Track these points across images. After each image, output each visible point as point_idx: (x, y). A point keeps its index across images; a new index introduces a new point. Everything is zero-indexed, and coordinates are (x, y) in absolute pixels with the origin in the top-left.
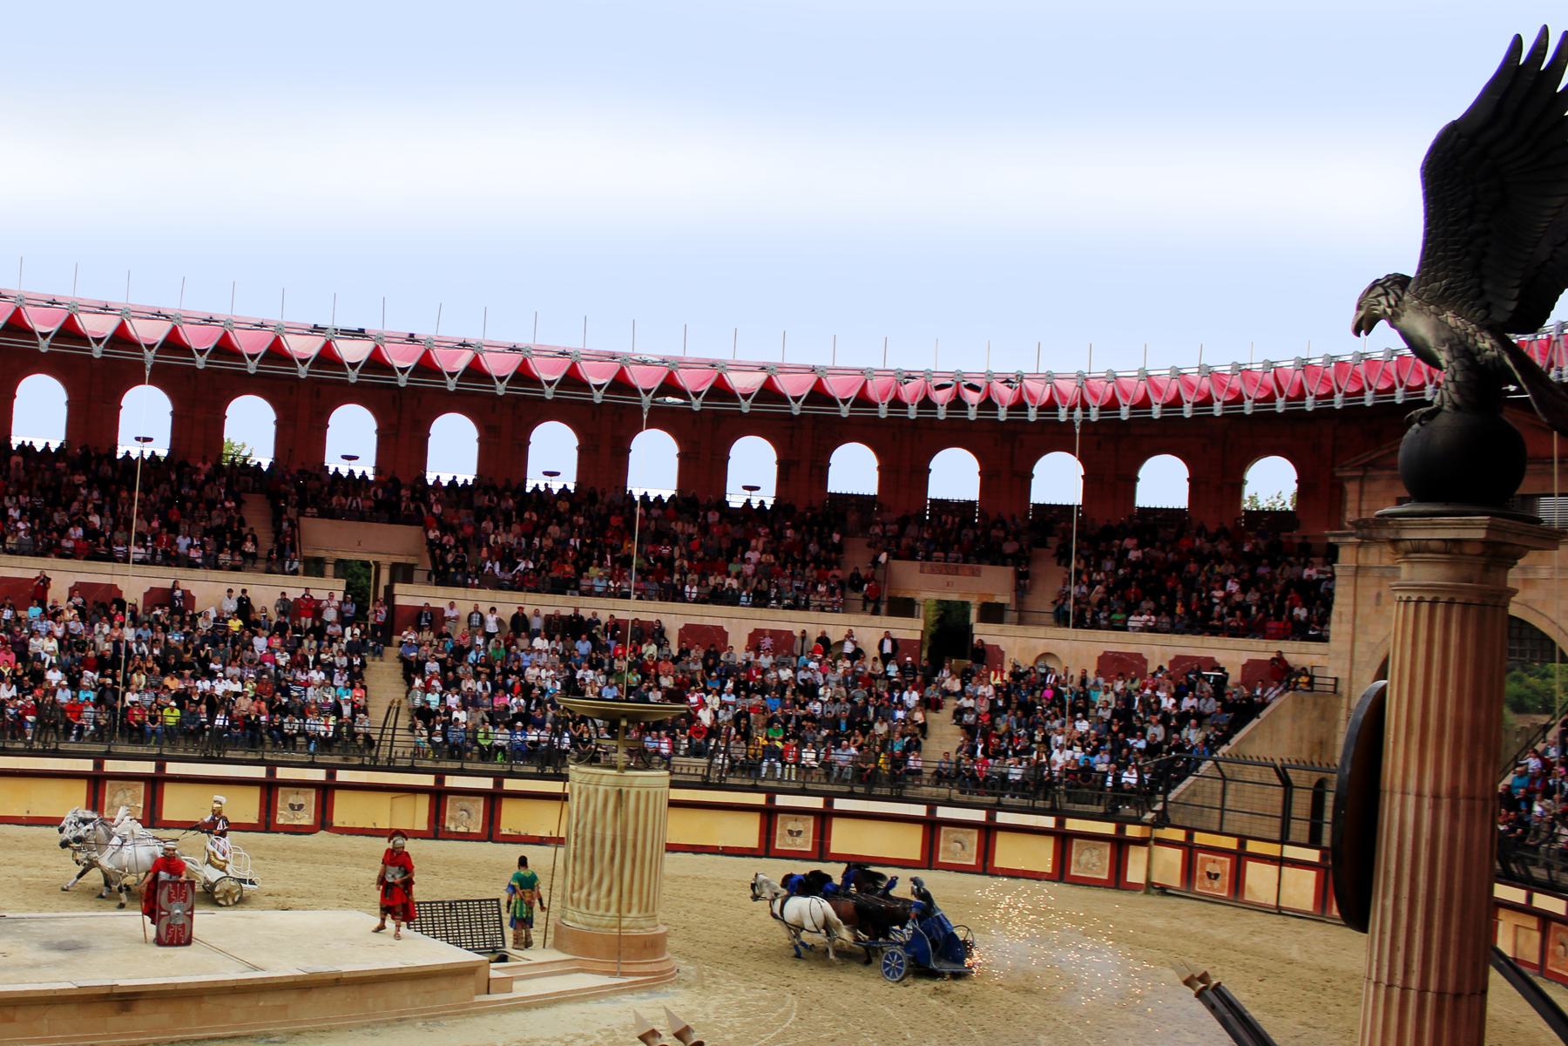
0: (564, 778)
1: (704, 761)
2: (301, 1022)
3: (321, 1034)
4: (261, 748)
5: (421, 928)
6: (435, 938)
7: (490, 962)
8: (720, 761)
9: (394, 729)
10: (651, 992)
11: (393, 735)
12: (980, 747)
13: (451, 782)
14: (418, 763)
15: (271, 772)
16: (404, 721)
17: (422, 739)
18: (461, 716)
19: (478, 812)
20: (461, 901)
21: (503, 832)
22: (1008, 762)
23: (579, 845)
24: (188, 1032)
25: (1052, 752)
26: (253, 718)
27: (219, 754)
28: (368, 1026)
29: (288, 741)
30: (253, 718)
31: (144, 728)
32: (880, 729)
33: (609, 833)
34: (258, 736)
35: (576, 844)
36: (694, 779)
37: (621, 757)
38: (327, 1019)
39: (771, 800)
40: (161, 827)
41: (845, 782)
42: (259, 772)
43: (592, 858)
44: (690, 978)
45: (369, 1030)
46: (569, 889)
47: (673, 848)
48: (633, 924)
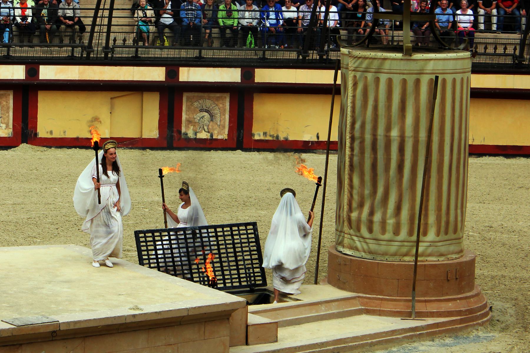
0: (335, 65)
5: (158, 263)
7: (248, 304)
9: (111, 9)
10: (457, 337)
11: (110, 17)
14: (143, 53)
19: (223, 113)
21: (257, 137)
33: (395, 133)
35: (352, 149)
36: (502, 60)
43: (374, 166)
44: (507, 317)
46: (346, 207)
48: (430, 250)
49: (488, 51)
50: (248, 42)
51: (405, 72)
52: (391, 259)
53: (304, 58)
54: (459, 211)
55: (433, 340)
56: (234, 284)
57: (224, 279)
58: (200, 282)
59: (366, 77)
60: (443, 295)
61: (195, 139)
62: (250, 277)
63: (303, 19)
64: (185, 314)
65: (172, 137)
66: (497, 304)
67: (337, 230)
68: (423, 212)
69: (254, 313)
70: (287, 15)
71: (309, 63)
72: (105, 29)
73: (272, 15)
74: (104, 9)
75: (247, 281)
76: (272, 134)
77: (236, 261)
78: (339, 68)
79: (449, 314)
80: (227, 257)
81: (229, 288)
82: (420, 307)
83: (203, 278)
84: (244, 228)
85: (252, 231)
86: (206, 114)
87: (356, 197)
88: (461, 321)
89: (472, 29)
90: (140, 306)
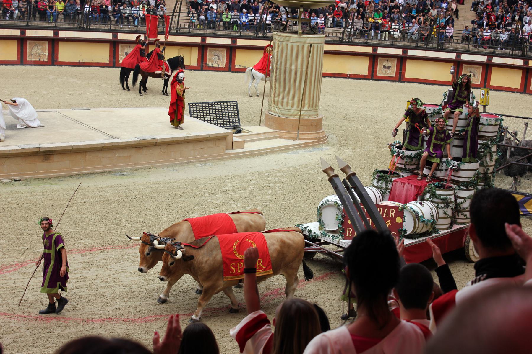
0: (271, 39)
1: (341, 30)
2: (137, 165)
3: (149, 170)
4: (109, 23)
5: (197, 116)
6: (204, 121)
7: (233, 133)
8: (349, 30)
9: (179, 13)
11: (179, 16)
12: (485, 22)
13: (210, 41)
14: (192, 31)
15: (115, 36)
16: (184, 9)
17: (195, 19)
18: (214, 6)
20: (217, 102)
22: (500, 30)
23: (278, 74)
24: (79, 170)
25: (524, 26)
26: (104, 7)
27: (87, 27)
28: (172, 166)
29: (121, 19)
30: (104, 7)
31: (46, 13)
32: (434, 12)
33: (293, 67)
34: (108, 16)
35: (276, 73)
36: (335, 39)
37: (298, 28)
38: (150, 163)
39: (375, 50)
40: (57, 65)
41: (413, 41)
42: (109, 36)
45: (172, 168)
46: (273, 96)
47: (325, 75)
48: (305, 114)
49: (330, 35)
50: (234, 28)
51: (299, 42)
52: (290, 117)
53: (257, 35)
54: (317, 99)
55: (305, 149)
56: (228, 125)
57: (224, 123)
58: (214, 124)
59: (283, 44)
60: (310, 132)
61: (212, 67)
62: (234, 122)
63: (257, 20)
64: (208, 136)
65: (203, 65)
66: (330, 136)
67: (269, 105)
68: (303, 99)
69: (235, 137)
70: (250, 18)
71: (259, 37)
72: (177, 21)
73: (244, 17)
74: (176, 12)
75: (233, 124)
76: (243, 66)
77: (229, 116)
78: (272, 40)
79: (312, 139)
80: (225, 114)
81: (226, 127)
82: (301, 136)
83: (215, 122)
84: (232, 103)
85: (235, 104)
86: (217, 57)
87: (277, 92)
88: (316, 142)
89: (324, 26)
90: (190, 133)
